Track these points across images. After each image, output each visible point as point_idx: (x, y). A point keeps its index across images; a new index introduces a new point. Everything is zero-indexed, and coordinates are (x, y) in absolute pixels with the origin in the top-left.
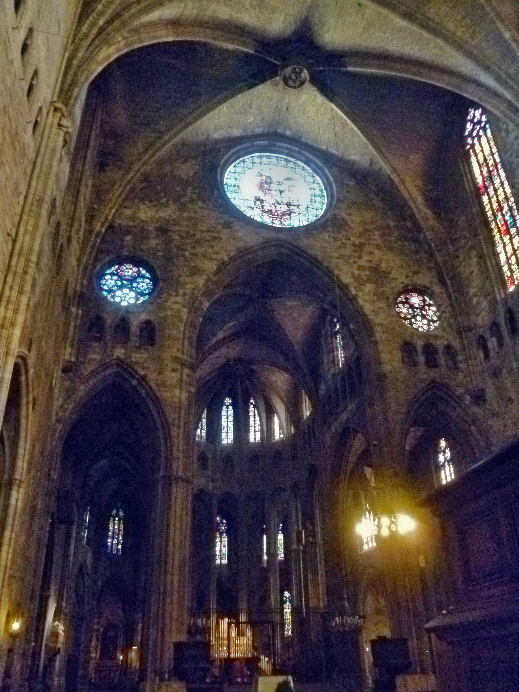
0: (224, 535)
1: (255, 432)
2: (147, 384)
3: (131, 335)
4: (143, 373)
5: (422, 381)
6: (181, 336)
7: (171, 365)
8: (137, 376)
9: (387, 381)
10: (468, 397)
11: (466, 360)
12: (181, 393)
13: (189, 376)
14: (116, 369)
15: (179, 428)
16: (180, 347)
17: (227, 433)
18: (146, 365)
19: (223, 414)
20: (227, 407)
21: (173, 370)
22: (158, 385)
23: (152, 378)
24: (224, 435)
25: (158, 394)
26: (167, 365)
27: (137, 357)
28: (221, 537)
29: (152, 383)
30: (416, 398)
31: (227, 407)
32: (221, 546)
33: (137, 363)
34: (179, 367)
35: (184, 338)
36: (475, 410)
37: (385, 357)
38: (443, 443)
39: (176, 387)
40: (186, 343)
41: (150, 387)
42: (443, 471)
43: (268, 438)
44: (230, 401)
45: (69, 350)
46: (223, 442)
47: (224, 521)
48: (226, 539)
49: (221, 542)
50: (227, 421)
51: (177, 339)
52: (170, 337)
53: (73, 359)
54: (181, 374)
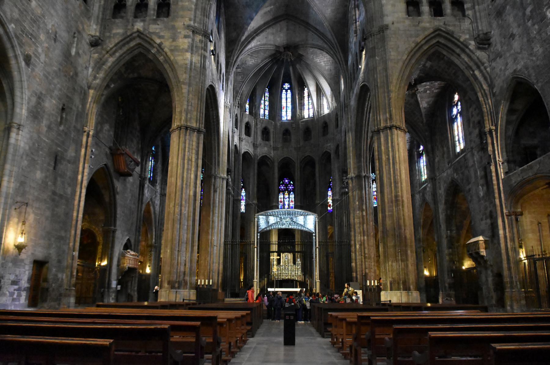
0: (292, 193)
1: (309, 109)
2: (163, 50)
3: (149, 10)
4: (158, 41)
5: (424, 29)
6: (193, 7)
7: (184, 32)
8: (155, 45)
9: (388, 32)
10: (473, 43)
11: (473, 7)
12: (191, 57)
13: (201, 41)
14: (138, 41)
15: (190, 85)
16: (192, 17)
17: (287, 111)
18: (162, 34)
19: (283, 97)
20: (286, 91)
21: (186, 37)
22: (172, 51)
23: (167, 45)
24: (284, 113)
25: (172, 58)
26: (180, 32)
27: (153, 28)
28: (289, 195)
29: (166, 50)
30: (418, 46)
31: (286, 91)
32: (289, 201)
33: (154, 33)
34: (191, 33)
35: (196, 9)
36: (480, 54)
37: (388, 9)
38: (456, 97)
39: (187, 51)
40: (199, 13)
41: (166, 53)
42: (456, 124)
43: (318, 112)
44: (289, 86)
45: (95, 27)
46: (283, 119)
47: (292, 183)
48: (293, 196)
49: (289, 198)
50: (287, 102)
51: (190, 10)
52: (183, 8)
53: (98, 34)
54: (193, 40)
